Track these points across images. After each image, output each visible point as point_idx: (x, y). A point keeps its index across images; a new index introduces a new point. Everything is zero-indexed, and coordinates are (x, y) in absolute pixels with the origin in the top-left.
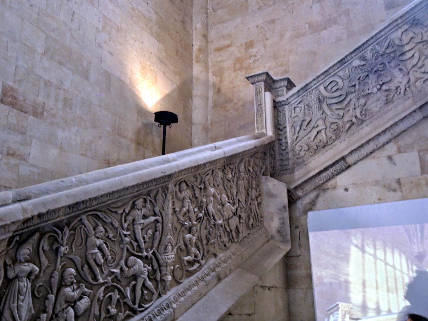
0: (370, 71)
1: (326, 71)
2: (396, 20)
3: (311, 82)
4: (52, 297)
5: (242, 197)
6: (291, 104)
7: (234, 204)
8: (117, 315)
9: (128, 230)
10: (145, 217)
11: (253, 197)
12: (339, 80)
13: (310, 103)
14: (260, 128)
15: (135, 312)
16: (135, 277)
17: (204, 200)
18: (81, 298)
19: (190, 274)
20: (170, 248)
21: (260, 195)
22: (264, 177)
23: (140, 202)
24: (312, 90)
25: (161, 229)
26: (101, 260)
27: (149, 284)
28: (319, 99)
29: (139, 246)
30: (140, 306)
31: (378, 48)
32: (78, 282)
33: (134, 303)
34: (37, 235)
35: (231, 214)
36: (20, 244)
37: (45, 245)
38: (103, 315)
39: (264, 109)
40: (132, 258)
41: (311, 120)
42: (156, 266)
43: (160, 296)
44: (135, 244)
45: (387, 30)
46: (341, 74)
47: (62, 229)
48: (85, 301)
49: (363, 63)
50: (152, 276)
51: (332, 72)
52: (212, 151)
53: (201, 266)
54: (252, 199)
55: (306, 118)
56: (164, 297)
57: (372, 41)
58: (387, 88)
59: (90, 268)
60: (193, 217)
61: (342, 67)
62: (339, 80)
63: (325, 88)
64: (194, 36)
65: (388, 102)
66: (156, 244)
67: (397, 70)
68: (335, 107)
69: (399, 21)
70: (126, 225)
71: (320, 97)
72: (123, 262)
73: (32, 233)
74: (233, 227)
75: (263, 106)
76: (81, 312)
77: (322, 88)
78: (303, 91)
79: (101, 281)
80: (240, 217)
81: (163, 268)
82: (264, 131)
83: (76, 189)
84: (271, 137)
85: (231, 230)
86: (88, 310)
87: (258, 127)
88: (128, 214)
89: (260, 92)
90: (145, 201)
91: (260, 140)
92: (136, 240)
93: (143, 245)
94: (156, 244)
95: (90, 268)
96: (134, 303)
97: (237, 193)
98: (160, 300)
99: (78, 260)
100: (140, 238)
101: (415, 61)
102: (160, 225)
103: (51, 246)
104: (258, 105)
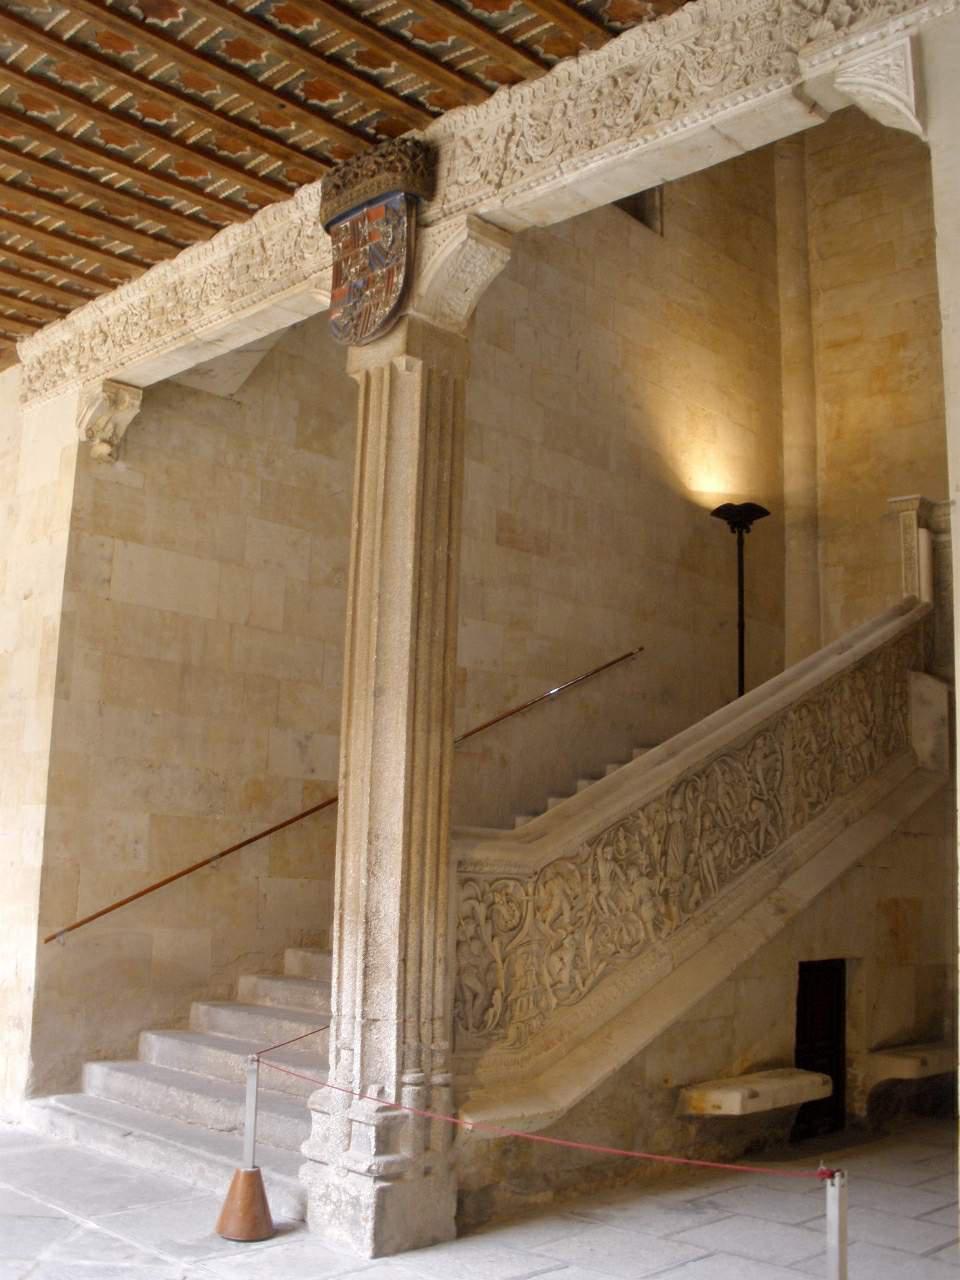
4: (697, 840)
5: (879, 710)
7: (867, 723)
8: (745, 859)
9: (750, 772)
10: (766, 756)
11: (897, 707)
14: (909, 588)
15: (759, 857)
16: (757, 823)
17: (828, 725)
18: (716, 842)
19: (811, 817)
20: (791, 789)
21: (906, 702)
22: (913, 673)
23: (760, 742)
25: (781, 768)
26: (729, 806)
27: (771, 829)
29: (761, 789)
30: (763, 852)
32: (714, 827)
33: (758, 848)
34: (684, 784)
35: (864, 738)
36: (675, 792)
37: (690, 794)
38: (734, 858)
39: (916, 557)
40: (756, 802)
42: (778, 810)
43: (781, 842)
44: (757, 786)
47: (699, 777)
48: (721, 845)
50: (774, 820)
52: (840, 654)
53: (823, 810)
54: (893, 710)
56: (786, 842)
59: (722, 812)
60: (814, 747)
64: (782, 316)
66: (776, 784)
70: (748, 768)
72: (747, 808)
73: (680, 784)
74: (865, 754)
75: (915, 551)
76: (717, 854)
79: (730, 826)
80: (875, 741)
81: (785, 813)
82: (917, 595)
83: (711, 736)
84: (927, 605)
85: (862, 759)
86: (722, 853)
87: (907, 588)
88: (749, 757)
89: (910, 527)
90: (765, 739)
91: (908, 616)
92: (758, 783)
93: (763, 787)
94: (776, 784)
95: (722, 812)
96: (758, 848)
97: (872, 706)
98: (782, 846)
99: (713, 806)
100: (761, 779)
102: (779, 764)
103: (694, 792)
104: (906, 549)
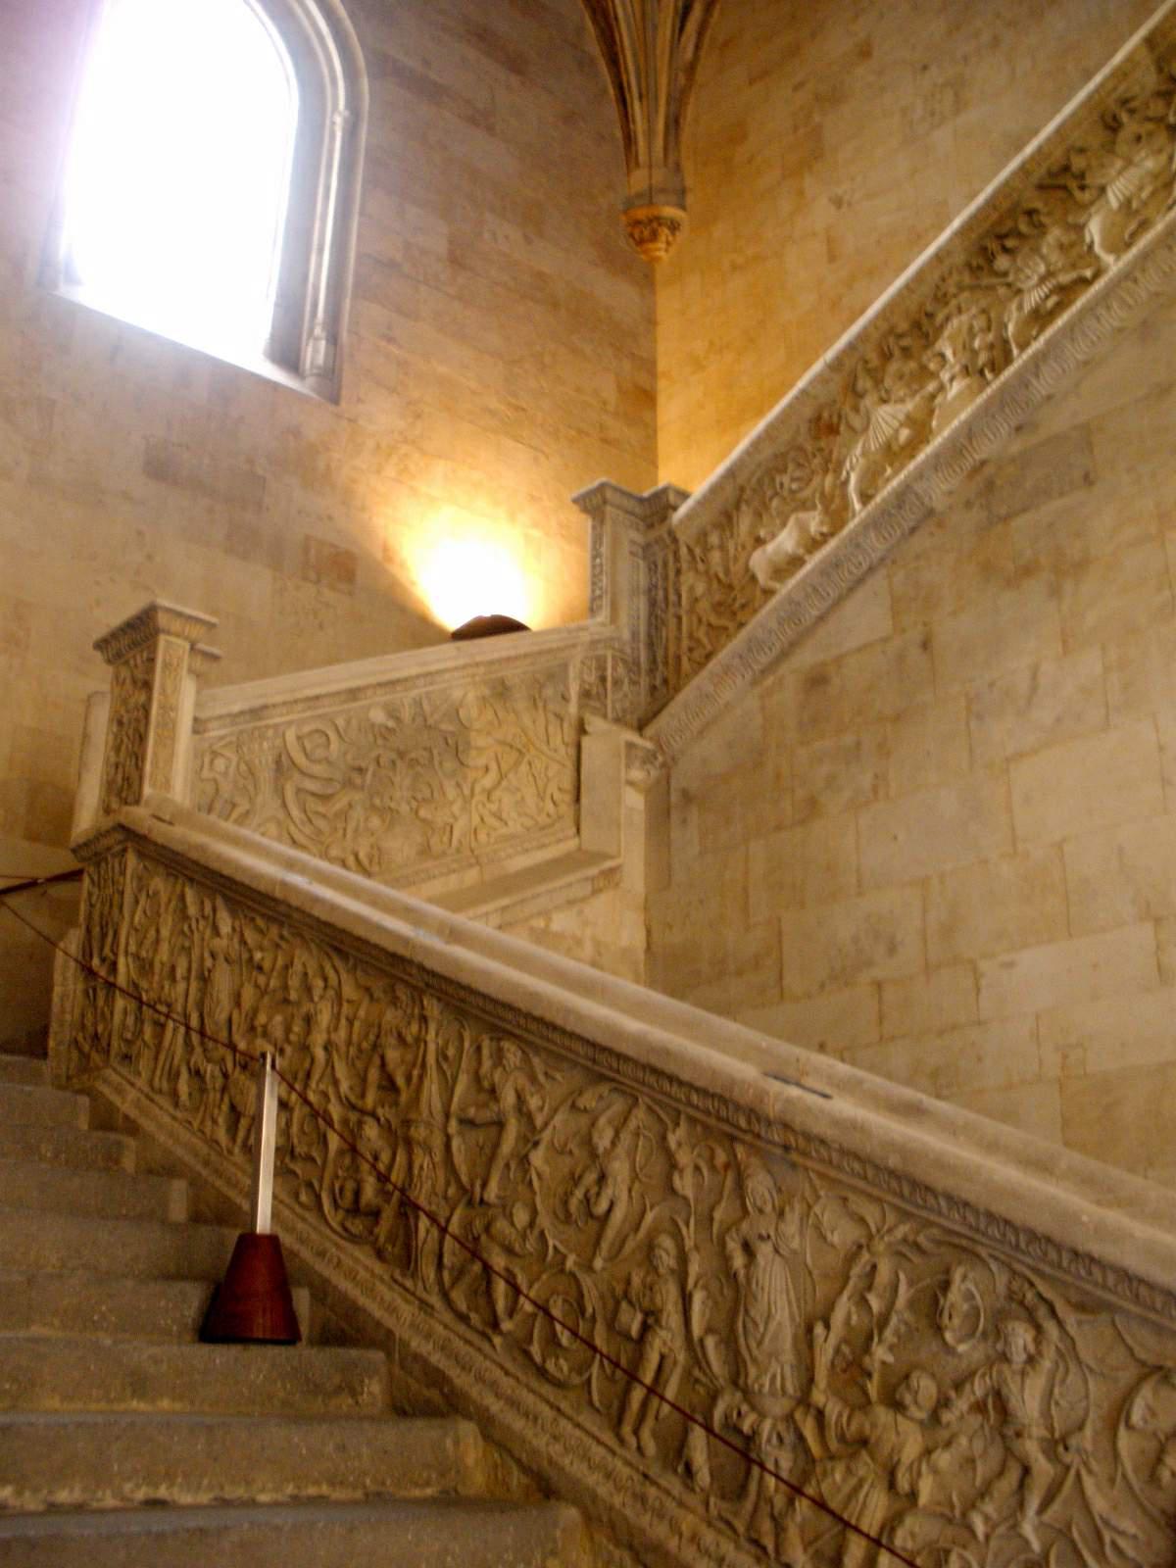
0: (401, 755)
1: (317, 698)
2: (477, 665)
3: (274, 706)
6: (206, 735)
12: (333, 736)
13: (257, 761)
24: (267, 727)
28: (278, 762)
31: (426, 707)
41: (248, 812)
45: (456, 674)
46: (340, 722)
49: (391, 724)
51: (324, 706)
55: (238, 799)
57: (422, 681)
58: (429, 817)
61: (346, 706)
62: (333, 736)
63: (299, 738)
65: (425, 851)
67: (453, 783)
68: (313, 805)
69: (482, 670)
71: (284, 758)
77: (291, 735)
78: (247, 717)
101: (488, 781)
